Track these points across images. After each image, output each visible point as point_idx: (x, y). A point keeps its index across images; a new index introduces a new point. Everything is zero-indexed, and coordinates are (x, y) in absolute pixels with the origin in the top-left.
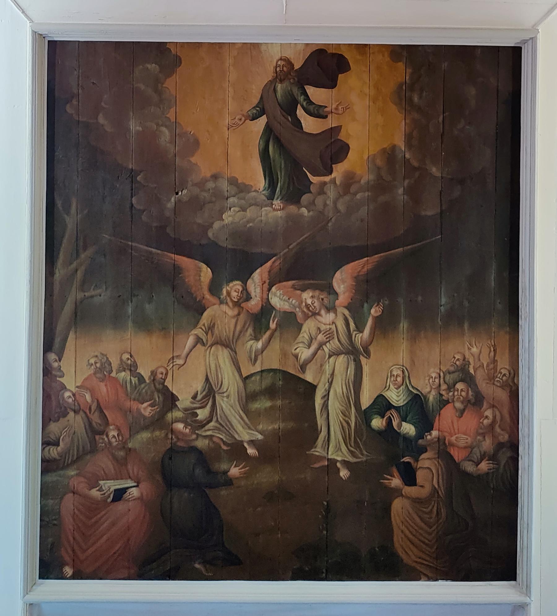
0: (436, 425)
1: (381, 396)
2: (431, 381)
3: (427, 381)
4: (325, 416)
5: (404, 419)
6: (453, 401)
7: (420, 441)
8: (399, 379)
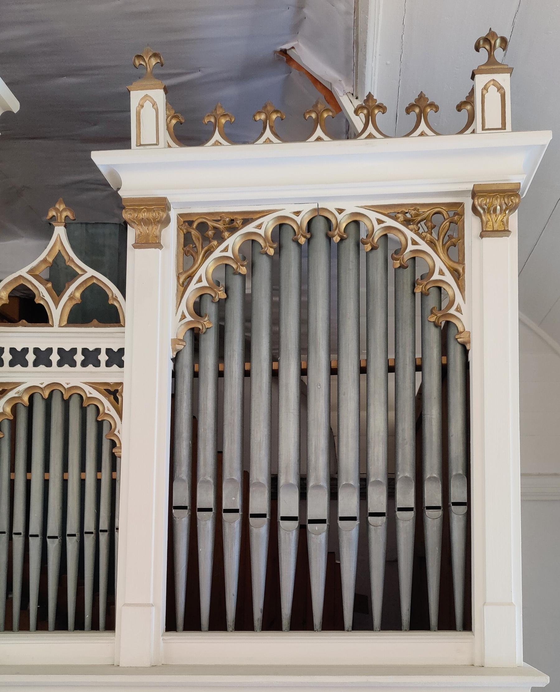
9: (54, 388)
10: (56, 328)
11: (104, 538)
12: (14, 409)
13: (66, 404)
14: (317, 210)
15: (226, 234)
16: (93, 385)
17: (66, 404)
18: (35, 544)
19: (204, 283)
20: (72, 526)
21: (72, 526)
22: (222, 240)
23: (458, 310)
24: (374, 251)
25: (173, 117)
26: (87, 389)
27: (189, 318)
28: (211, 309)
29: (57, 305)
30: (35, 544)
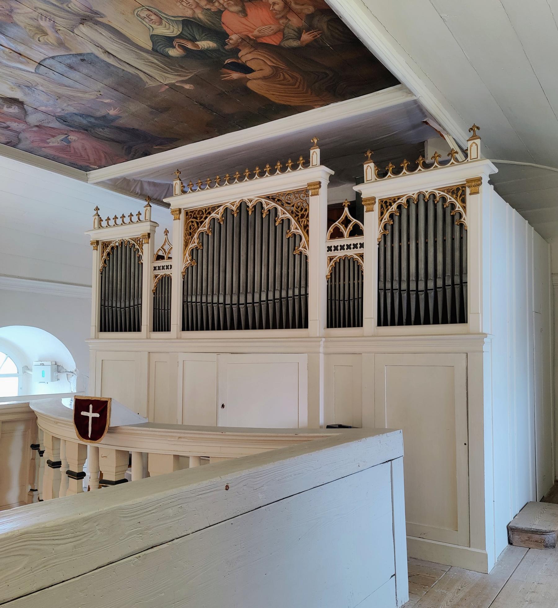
0: (228, 31)
1: (152, 36)
2: (185, 4)
3: (181, 6)
4: (127, 66)
5: (193, 40)
6: (225, 9)
7: (227, 47)
8: (153, 17)
9: (346, 256)
10: (346, 238)
11: (360, 300)
12: (335, 264)
13: (349, 260)
14: (420, 192)
15: (392, 204)
16: (356, 254)
17: (349, 260)
18: (342, 303)
19: (386, 220)
20: (351, 297)
21: (351, 297)
22: (391, 205)
23: (464, 219)
24: (438, 203)
25: (377, 170)
26: (354, 256)
27: (382, 231)
28: (389, 227)
29: (346, 231)
30: (342, 303)
